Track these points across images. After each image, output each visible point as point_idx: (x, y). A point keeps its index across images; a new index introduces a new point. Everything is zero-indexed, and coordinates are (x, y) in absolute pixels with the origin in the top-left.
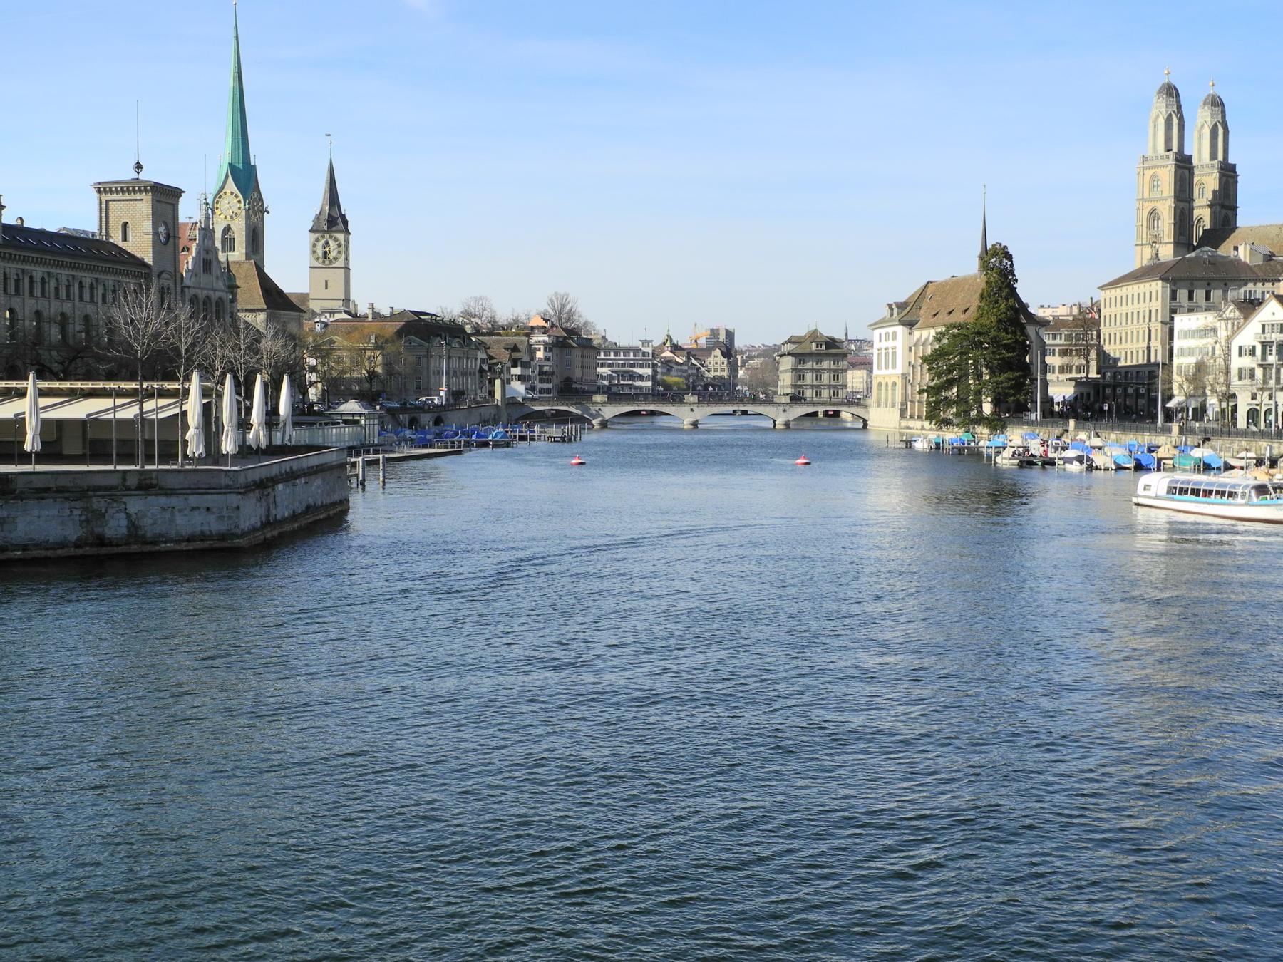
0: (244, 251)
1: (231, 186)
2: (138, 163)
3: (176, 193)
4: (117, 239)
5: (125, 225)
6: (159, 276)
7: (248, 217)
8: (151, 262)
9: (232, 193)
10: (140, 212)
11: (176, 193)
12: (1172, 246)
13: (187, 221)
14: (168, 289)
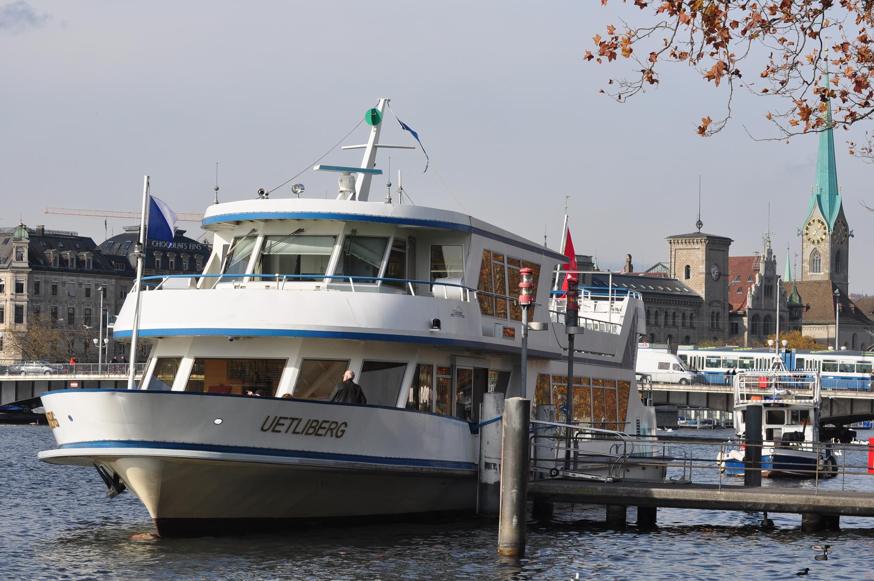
0: (827, 271)
1: (818, 215)
2: (700, 221)
3: (727, 242)
4: (681, 276)
5: (688, 267)
6: (710, 305)
7: (833, 241)
8: (703, 295)
9: (819, 221)
10: (697, 256)
11: (727, 242)
12: (826, 337)
13: (754, 255)
14: (718, 314)
